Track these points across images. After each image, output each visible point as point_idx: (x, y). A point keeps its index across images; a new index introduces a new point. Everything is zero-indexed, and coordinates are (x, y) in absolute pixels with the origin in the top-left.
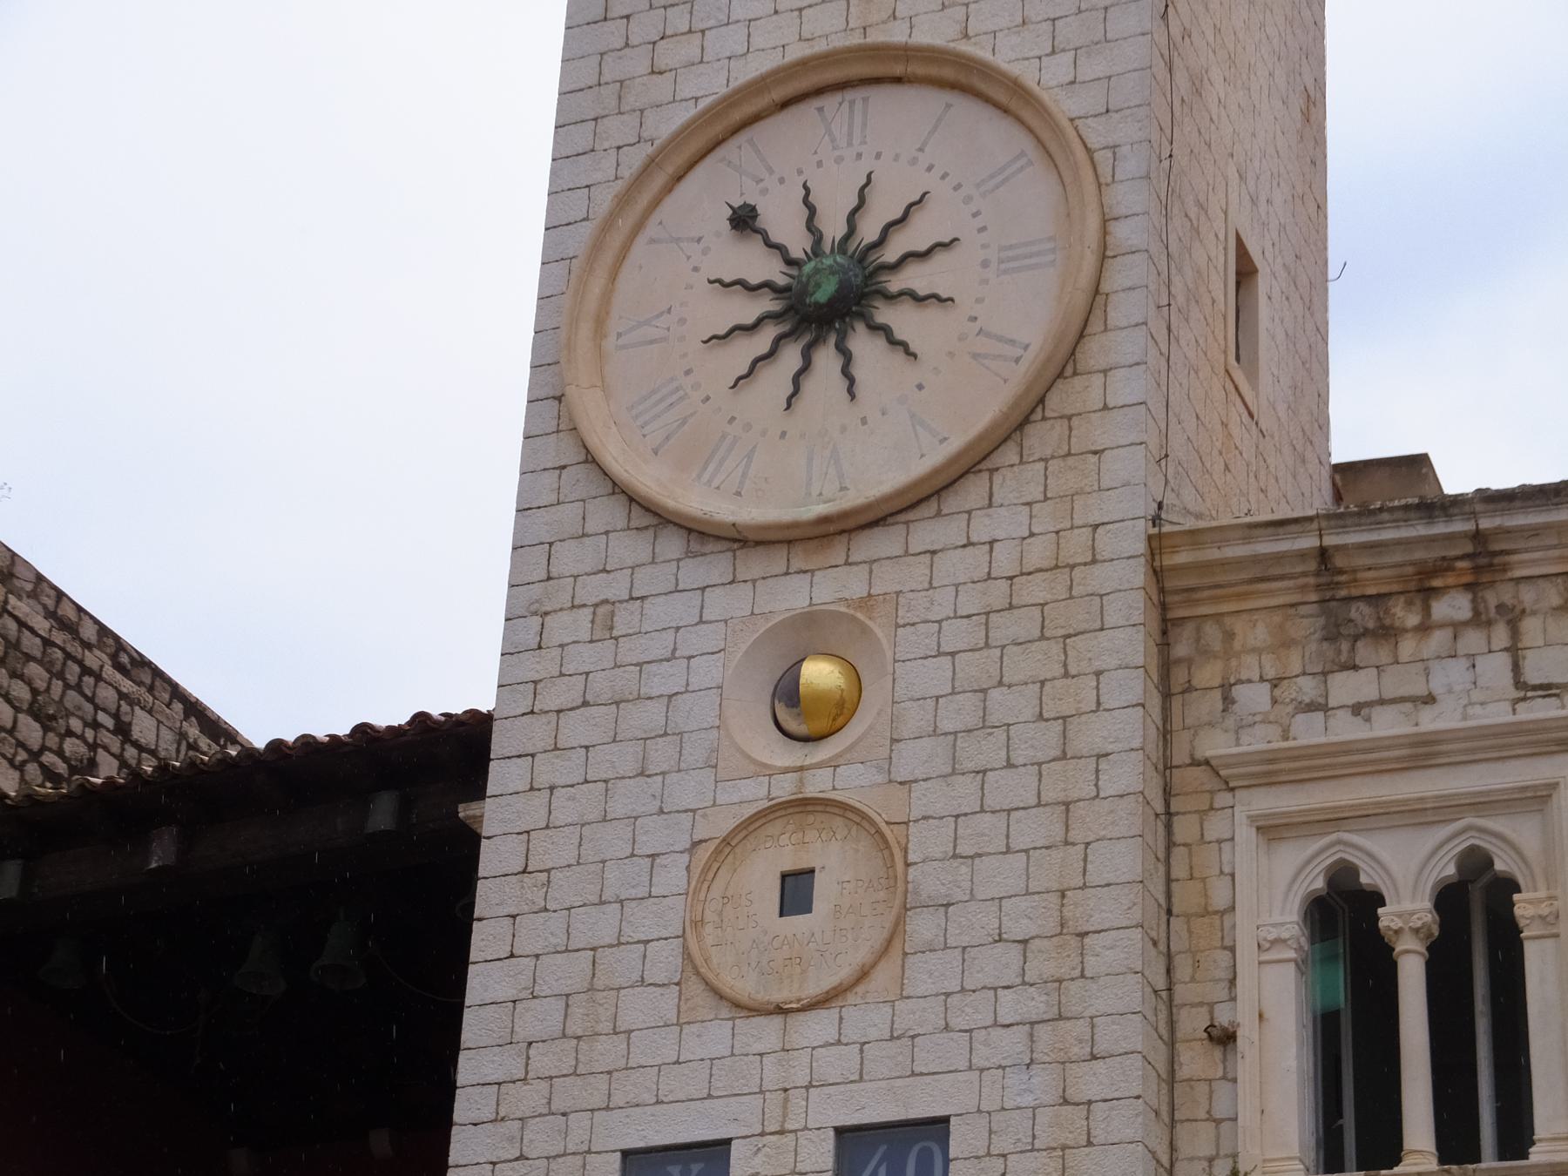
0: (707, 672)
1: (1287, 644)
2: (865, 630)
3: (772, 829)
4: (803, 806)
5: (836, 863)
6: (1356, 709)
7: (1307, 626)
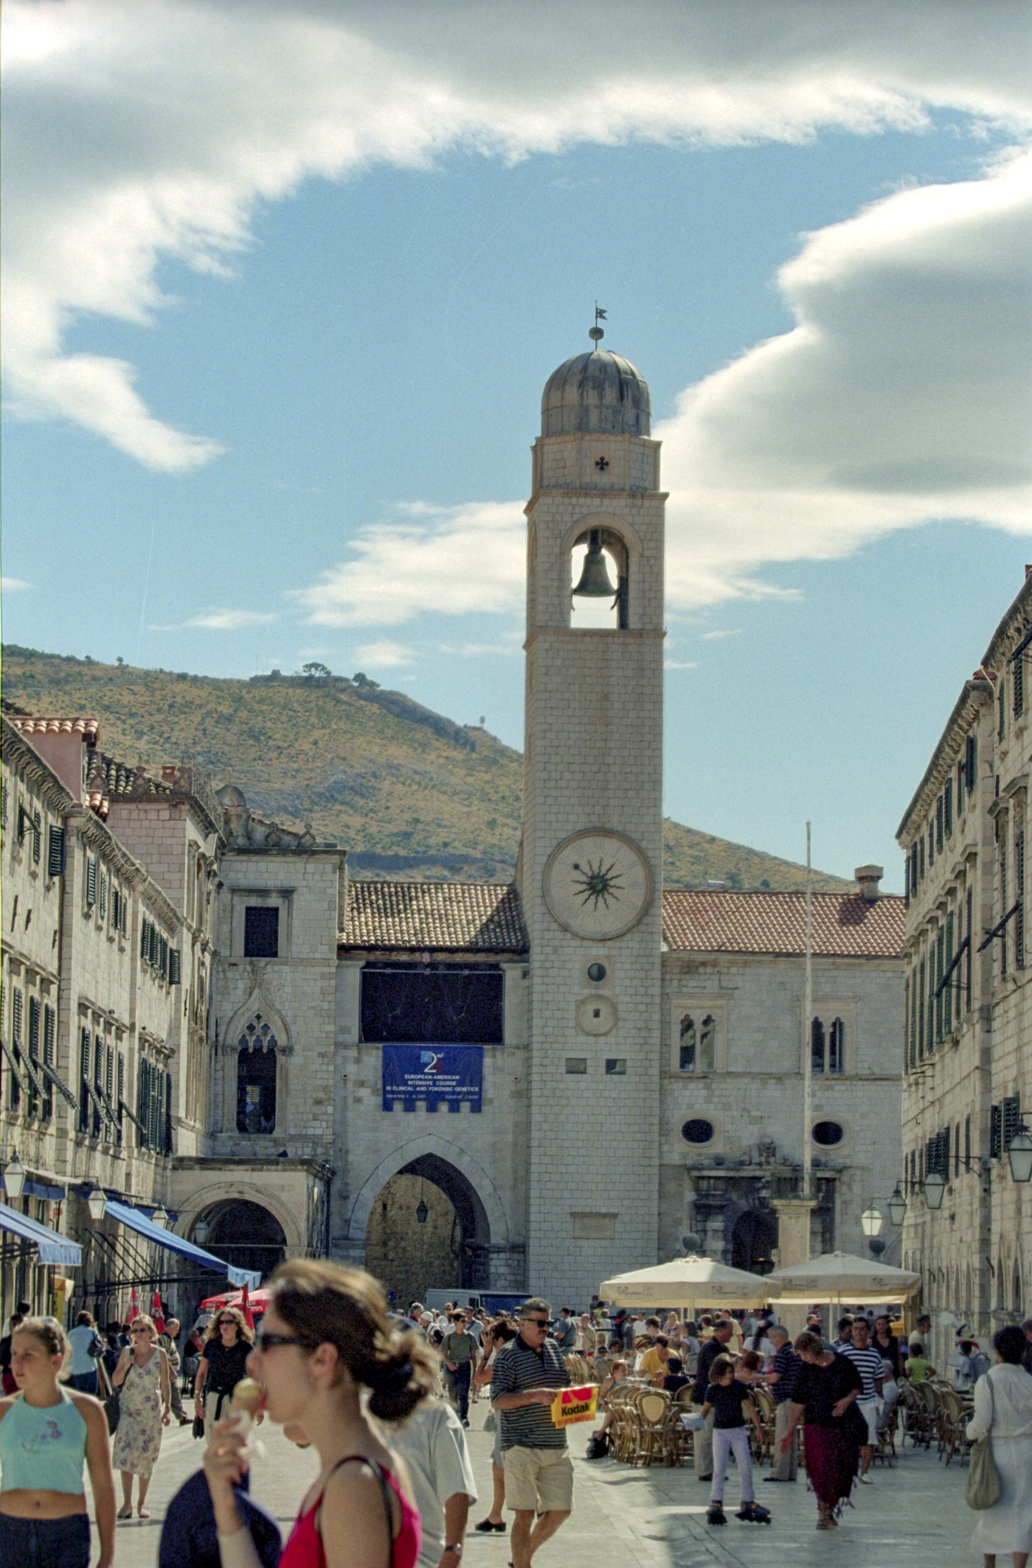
4: (599, 997)
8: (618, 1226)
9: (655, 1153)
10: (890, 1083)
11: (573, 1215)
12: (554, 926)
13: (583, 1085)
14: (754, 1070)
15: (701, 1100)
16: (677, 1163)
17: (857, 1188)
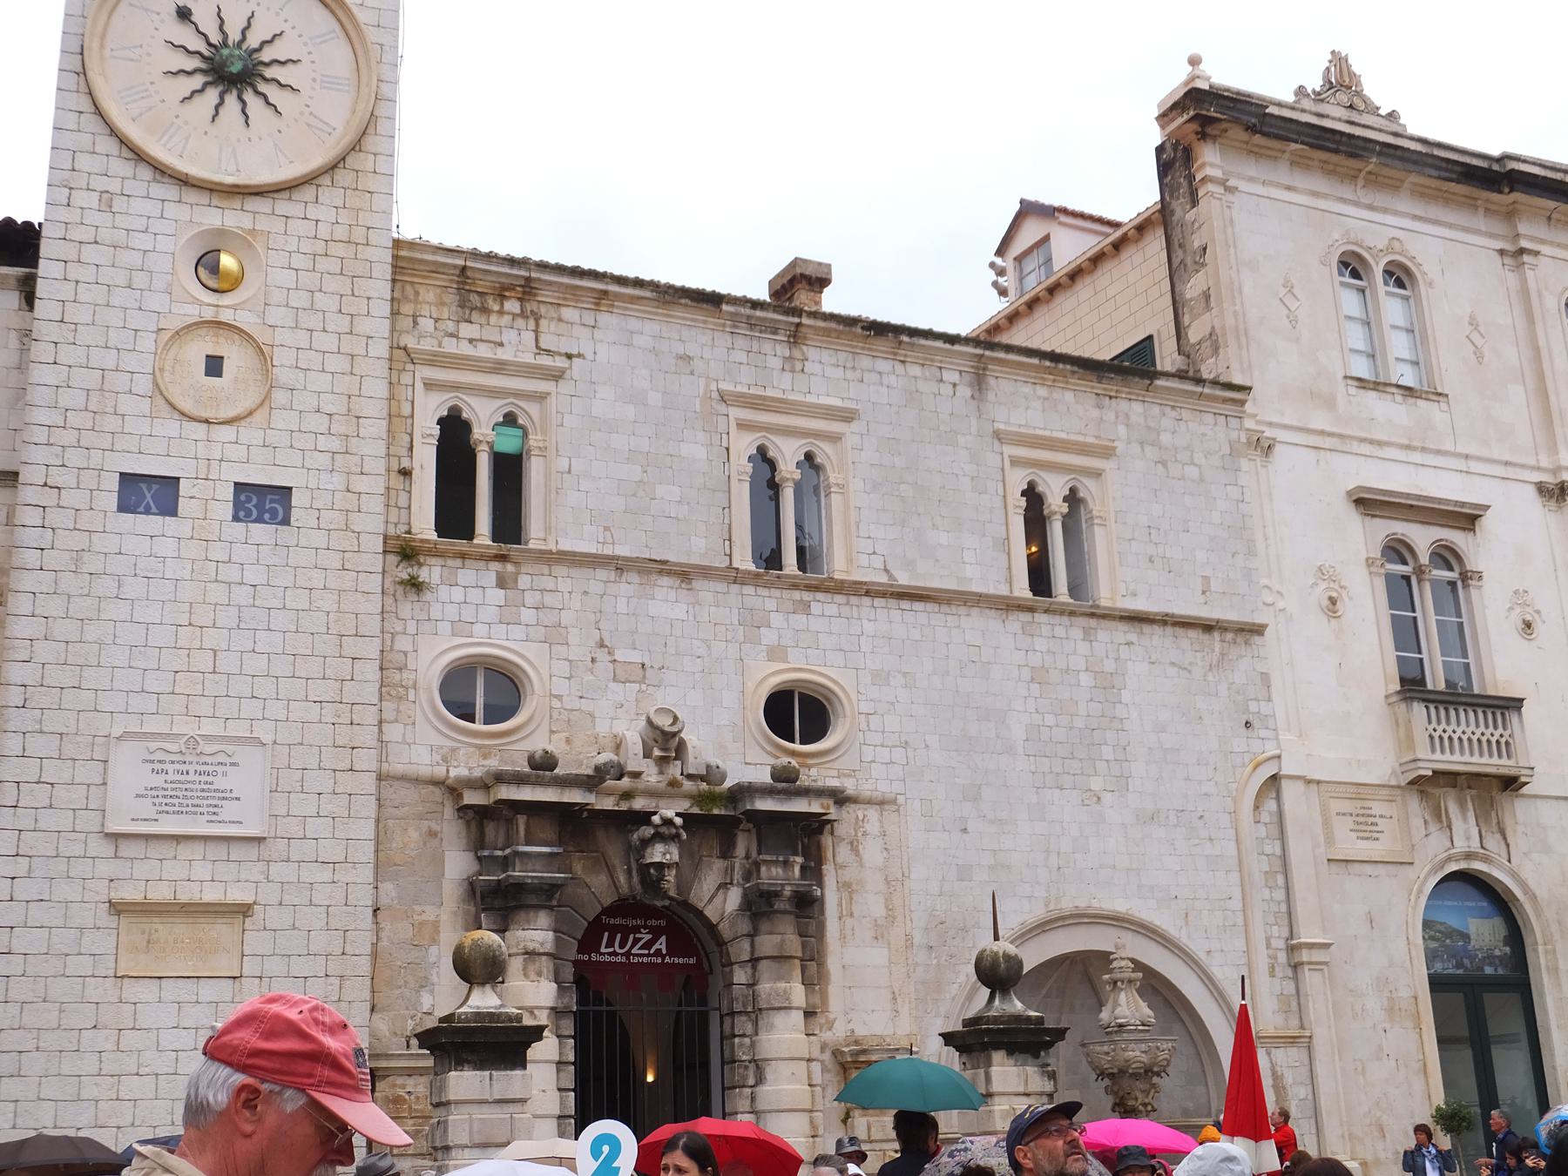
0: (165, 244)
1: (443, 304)
2: (250, 245)
3: (200, 332)
5: (236, 358)
6: (471, 341)
7: (451, 298)
8: (255, 941)
9: (368, 736)
10: (930, 606)
11: (118, 908)
12: (107, 145)
13: (167, 547)
14: (623, 551)
15: (490, 613)
16: (425, 771)
17: (872, 852)
